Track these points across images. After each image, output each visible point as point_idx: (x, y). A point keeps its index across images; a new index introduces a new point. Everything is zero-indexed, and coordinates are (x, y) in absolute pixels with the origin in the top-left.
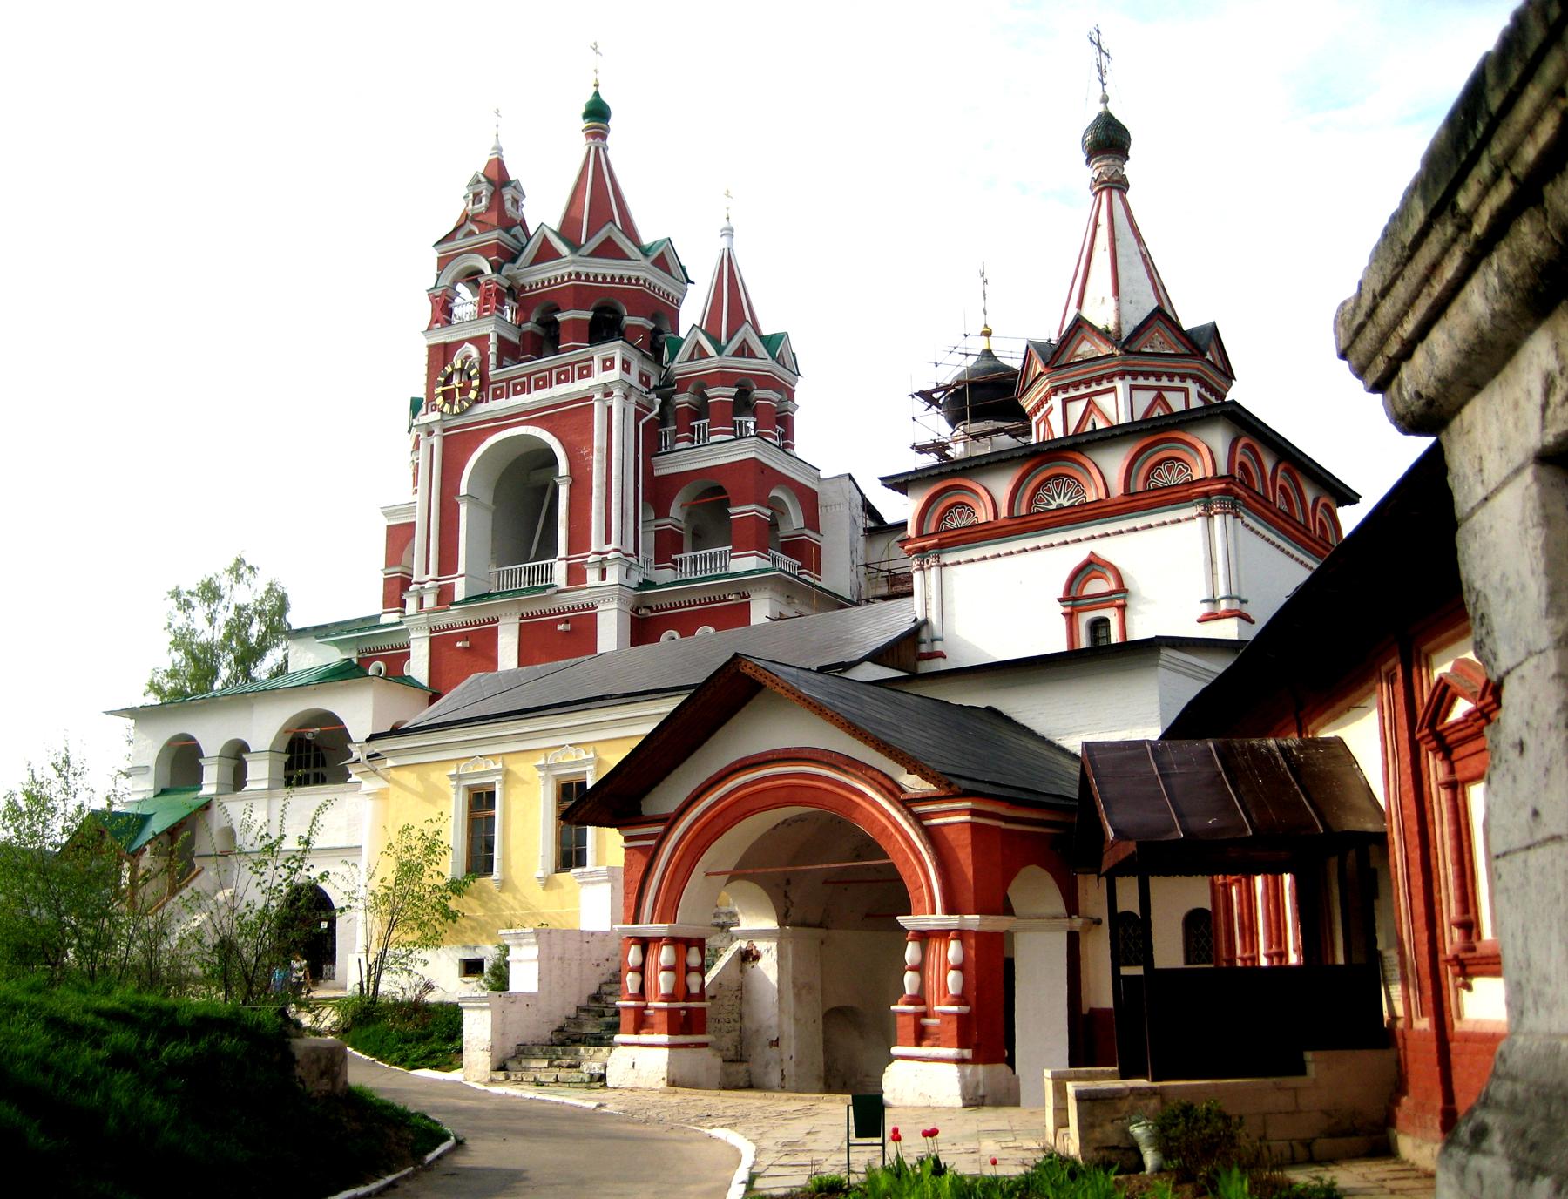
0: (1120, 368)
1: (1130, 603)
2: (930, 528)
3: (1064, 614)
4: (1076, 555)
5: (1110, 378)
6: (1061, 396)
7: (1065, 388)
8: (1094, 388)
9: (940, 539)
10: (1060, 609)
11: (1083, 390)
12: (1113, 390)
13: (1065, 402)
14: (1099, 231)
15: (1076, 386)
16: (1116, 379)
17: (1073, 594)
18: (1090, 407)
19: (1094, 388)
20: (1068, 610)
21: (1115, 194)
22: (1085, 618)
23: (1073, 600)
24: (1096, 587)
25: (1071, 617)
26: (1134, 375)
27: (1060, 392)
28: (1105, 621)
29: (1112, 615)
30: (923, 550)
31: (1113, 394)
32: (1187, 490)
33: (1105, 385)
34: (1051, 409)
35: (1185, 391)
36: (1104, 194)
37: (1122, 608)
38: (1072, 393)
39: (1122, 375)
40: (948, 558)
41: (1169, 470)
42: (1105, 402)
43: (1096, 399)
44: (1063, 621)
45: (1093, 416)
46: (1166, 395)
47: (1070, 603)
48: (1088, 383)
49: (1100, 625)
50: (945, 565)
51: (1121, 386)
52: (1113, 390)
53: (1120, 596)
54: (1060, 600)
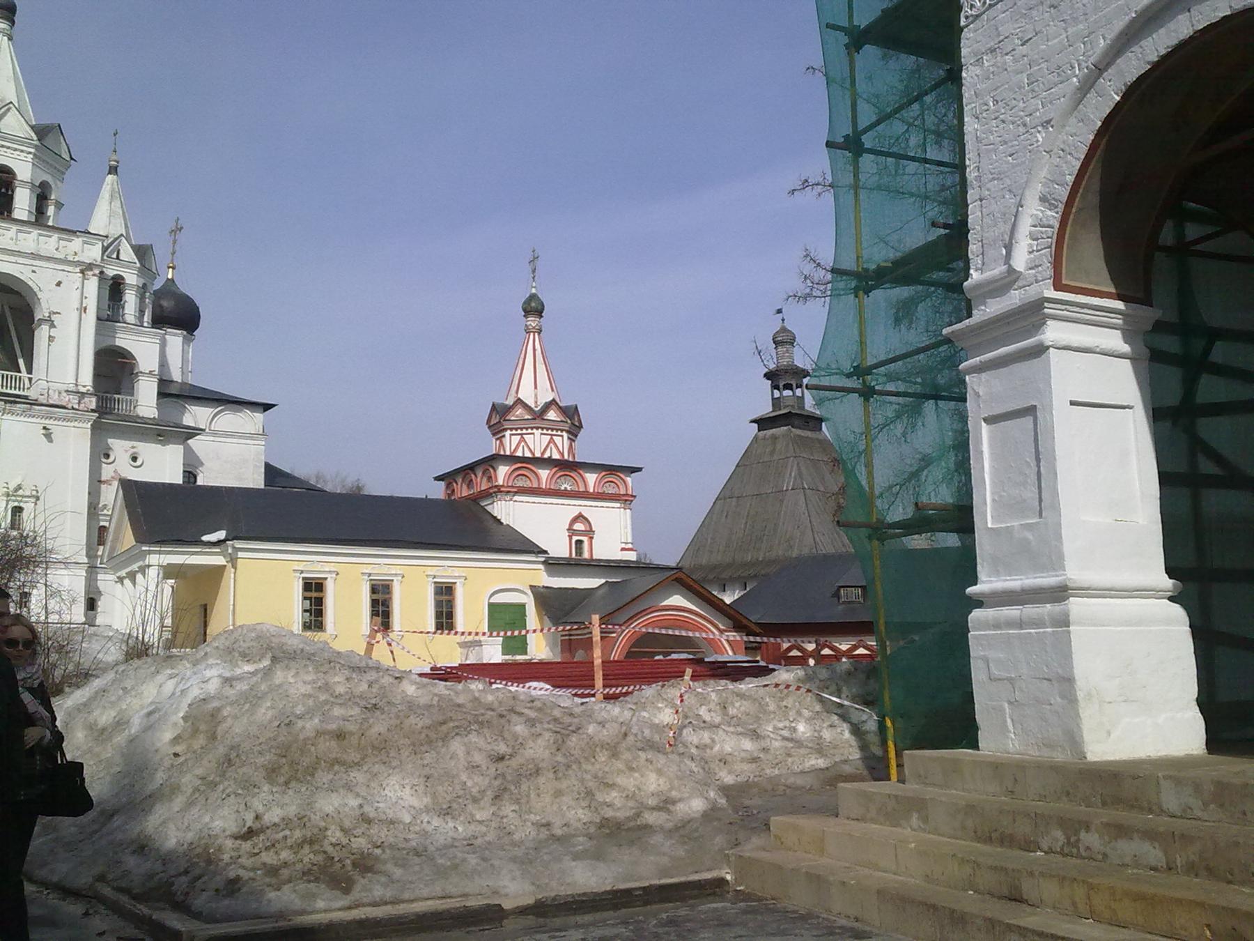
4: (574, 512)
5: (562, 431)
6: (540, 431)
7: (542, 429)
8: (554, 432)
11: (550, 432)
12: (562, 436)
14: (537, 352)
15: (548, 429)
19: (554, 432)
21: (536, 334)
22: (575, 538)
23: (572, 531)
24: (579, 526)
25: (570, 537)
29: (585, 539)
31: (561, 438)
33: (559, 433)
36: (532, 334)
37: (592, 538)
38: (545, 431)
40: (516, 498)
42: (557, 440)
44: (568, 538)
46: (554, 437)
49: (579, 543)
50: (516, 501)
52: (562, 436)
53: (590, 532)
54: (568, 530)
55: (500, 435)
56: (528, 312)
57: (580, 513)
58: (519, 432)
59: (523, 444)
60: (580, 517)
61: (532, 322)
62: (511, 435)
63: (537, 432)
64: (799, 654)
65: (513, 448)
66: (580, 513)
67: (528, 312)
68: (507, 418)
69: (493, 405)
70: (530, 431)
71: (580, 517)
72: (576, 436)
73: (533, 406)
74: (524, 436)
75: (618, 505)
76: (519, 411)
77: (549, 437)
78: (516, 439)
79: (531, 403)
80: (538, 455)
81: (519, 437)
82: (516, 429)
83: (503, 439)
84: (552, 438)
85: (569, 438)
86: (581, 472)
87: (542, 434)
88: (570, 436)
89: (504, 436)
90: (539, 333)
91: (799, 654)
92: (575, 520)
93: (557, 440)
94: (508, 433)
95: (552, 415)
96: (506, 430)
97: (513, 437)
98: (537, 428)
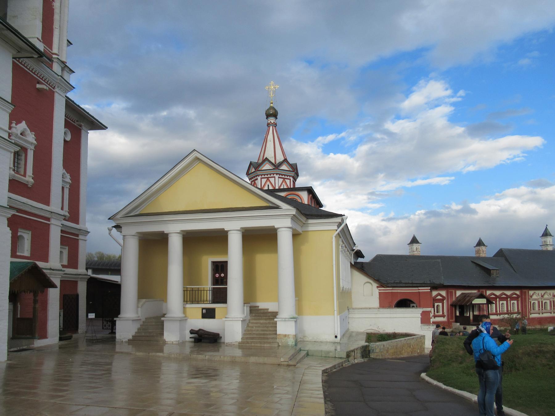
5: (290, 176)
6: (278, 176)
7: (280, 174)
8: (286, 177)
11: (283, 177)
15: (282, 175)
16: (291, 177)
19: (286, 177)
27: (278, 175)
31: (289, 180)
33: (288, 177)
35: (290, 179)
38: (281, 176)
45: (284, 183)
48: (285, 175)
52: (290, 179)
56: (268, 116)
59: (268, 183)
61: (272, 120)
62: (261, 178)
63: (277, 177)
65: (262, 187)
67: (268, 116)
68: (260, 169)
69: (251, 162)
70: (272, 175)
73: (274, 163)
74: (269, 179)
76: (267, 167)
78: (264, 181)
79: (273, 161)
80: (277, 188)
81: (266, 179)
82: (264, 175)
83: (256, 181)
84: (284, 180)
87: (279, 177)
89: (257, 179)
90: (275, 127)
93: (288, 181)
94: (259, 178)
95: (284, 167)
96: (258, 175)
97: (262, 179)
98: (277, 174)
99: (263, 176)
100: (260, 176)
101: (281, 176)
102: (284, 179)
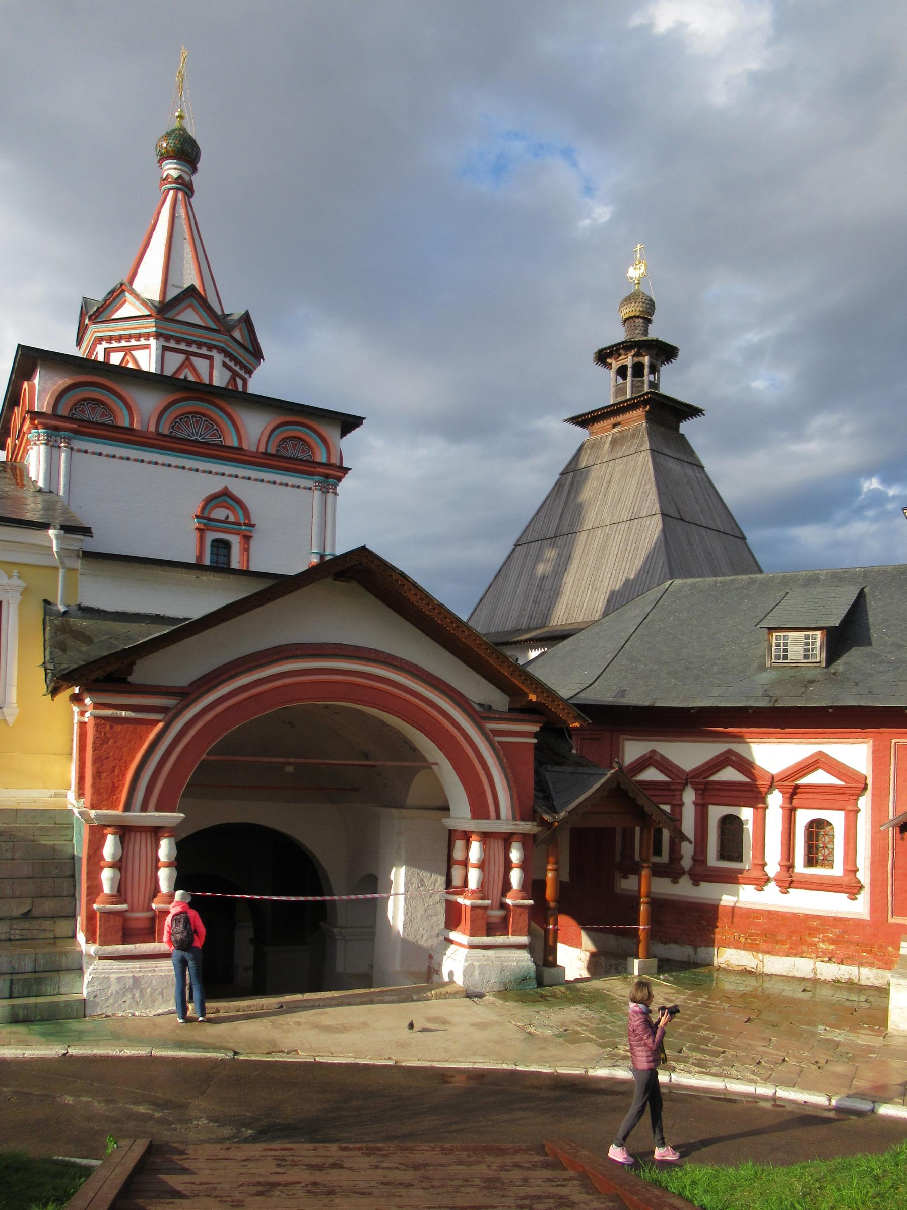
0: (221, 345)
1: (255, 536)
2: (63, 411)
3: (197, 529)
5: (210, 347)
8: (194, 349)
9: (79, 426)
10: (195, 523)
11: (183, 346)
12: (210, 358)
13: (165, 349)
15: (178, 340)
17: (205, 514)
18: (187, 362)
19: (194, 349)
20: (202, 527)
22: (211, 536)
23: (205, 522)
26: (227, 354)
28: (227, 545)
29: (235, 541)
30: (56, 429)
31: (207, 362)
32: (315, 468)
33: (204, 351)
34: (147, 347)
37: (247, 538)
38: (172, 344)
39: (221, 350)
40: (78, 444)
41: (294, 446)
42: (201, 365)
43: (193, 359)
44: (195, 536)
45: (187, 370)
47: (205, 521)
48: (189, 343)
49: (222, 547)
51: (218, 358)
52: (210, 358)
54: (197, 517)
55: (95, 354)
57: (226, 488)
58: (124, 343)
60: (224, 497)
64: (661, 777)
66: (226, 488)
70: (143, 342)
71: (224, 497)
72: (250, 372)
75: (310, 483)
77: (182, 357)
84: (187, 359)
85: (225, 365)
86: (230, 409)
88: (227, 360)
91: (661, 777)
92: (213, 500)
99: (115, 344)
100: (105, 345)
101: (172, 344)
102: (189, 354)
